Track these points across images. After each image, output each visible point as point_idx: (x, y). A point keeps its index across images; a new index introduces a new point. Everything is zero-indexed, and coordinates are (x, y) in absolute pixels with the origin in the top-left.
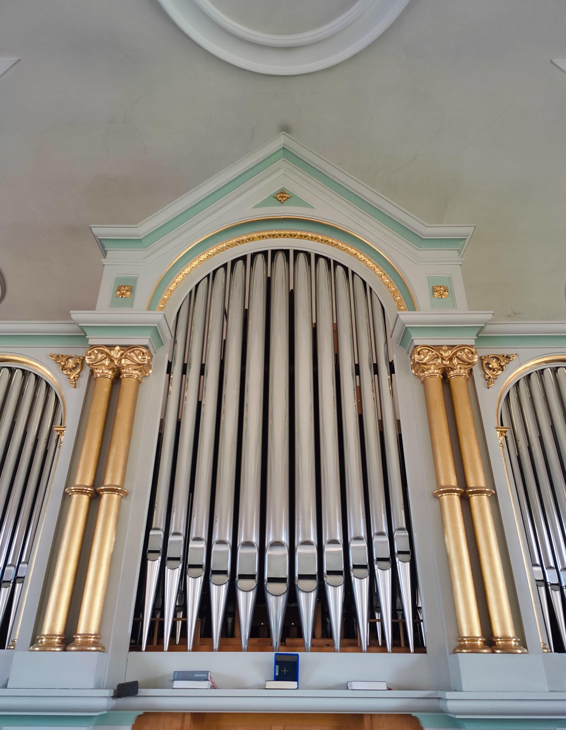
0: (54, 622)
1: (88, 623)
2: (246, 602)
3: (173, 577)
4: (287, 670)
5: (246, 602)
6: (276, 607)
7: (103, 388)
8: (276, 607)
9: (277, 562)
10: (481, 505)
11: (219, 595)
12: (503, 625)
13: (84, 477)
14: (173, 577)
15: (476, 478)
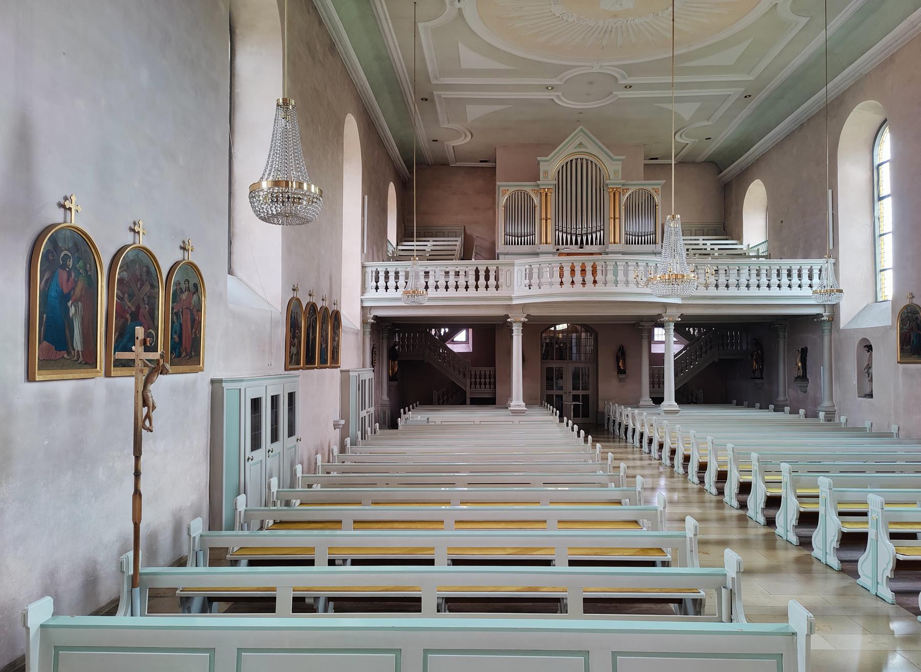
0: (544, 240)
1: (549, 240)
2: (574, 238)
3: (560, 234)
4: (581, 248)
5: (574, 238)
6: (579, 239)
7: (544, 197)
8: (579, 239)
9: (579, 231)
10: (617, 221)
11: (569, 237)
12: (617, 240)
13: (544, 216)
14: (560, 234)
15: (617, 216)
